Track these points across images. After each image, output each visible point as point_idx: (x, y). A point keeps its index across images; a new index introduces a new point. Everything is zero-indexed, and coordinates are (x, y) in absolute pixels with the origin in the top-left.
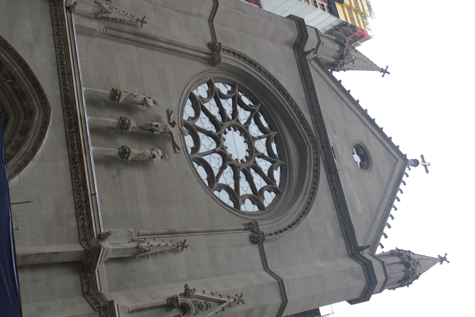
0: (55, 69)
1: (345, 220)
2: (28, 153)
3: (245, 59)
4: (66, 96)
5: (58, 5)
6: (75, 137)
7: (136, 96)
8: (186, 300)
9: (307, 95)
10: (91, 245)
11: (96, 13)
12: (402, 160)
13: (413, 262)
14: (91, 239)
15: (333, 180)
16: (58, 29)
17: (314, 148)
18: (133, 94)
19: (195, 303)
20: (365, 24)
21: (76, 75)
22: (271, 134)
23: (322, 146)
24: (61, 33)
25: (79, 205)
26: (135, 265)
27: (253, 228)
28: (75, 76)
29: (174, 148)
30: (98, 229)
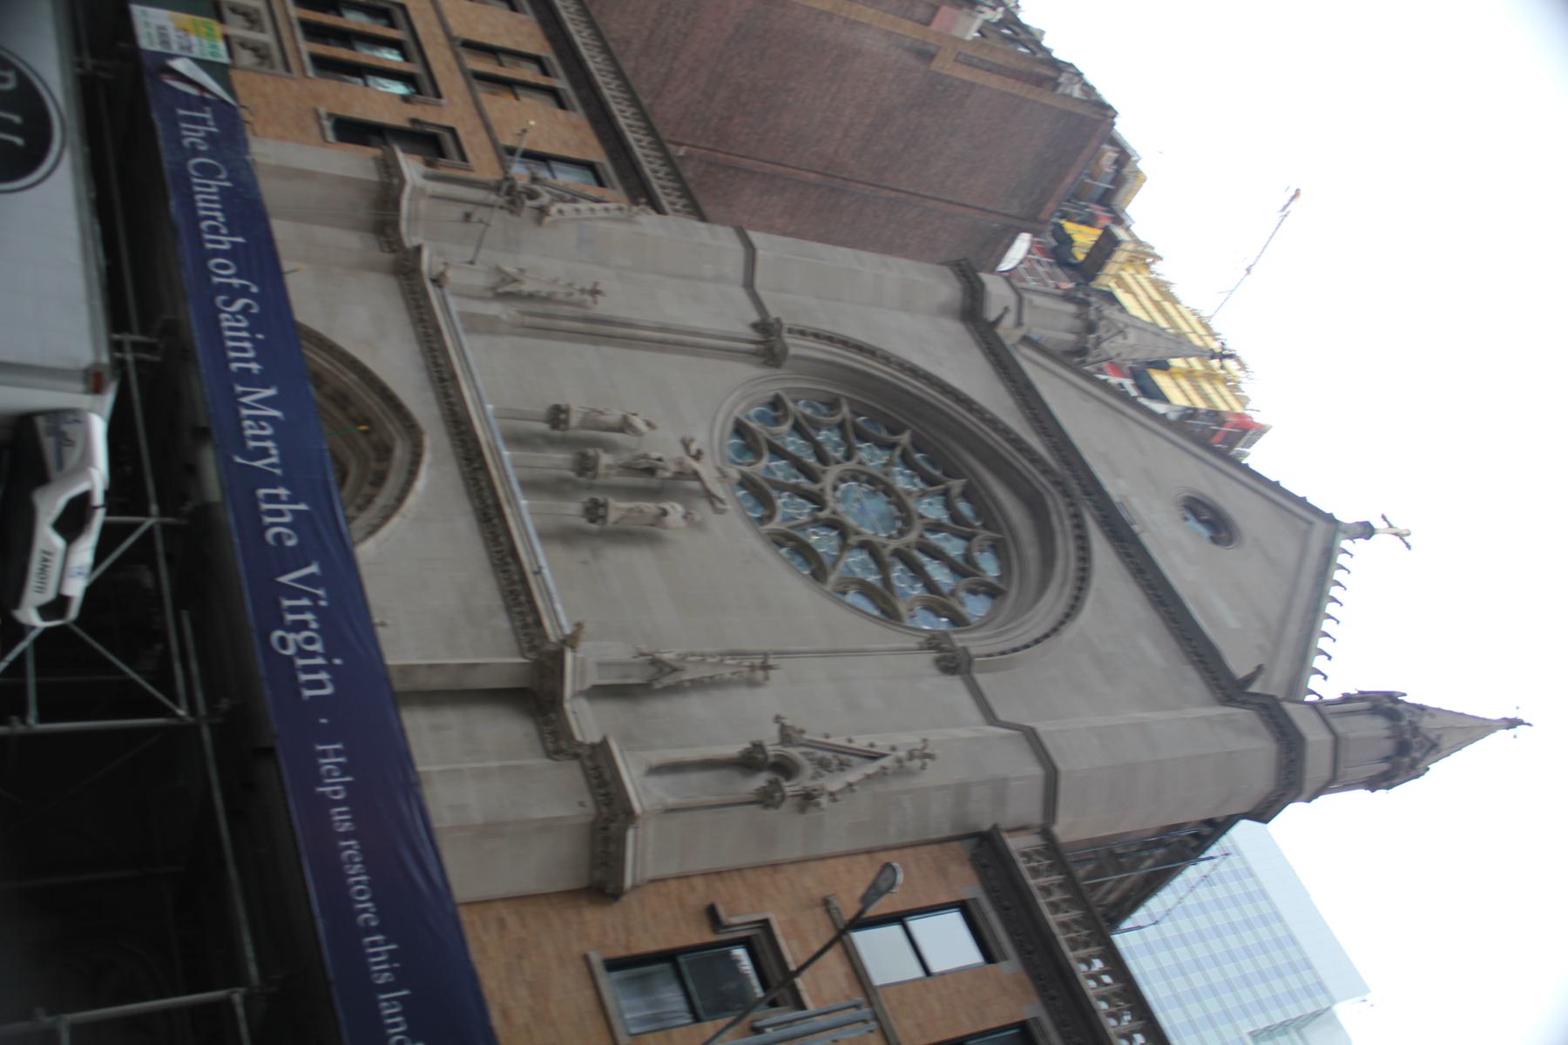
0: (423, 376)
3: (846, 343)
20: (1243, 401)
26: (658, 708)
29: (712, 503)
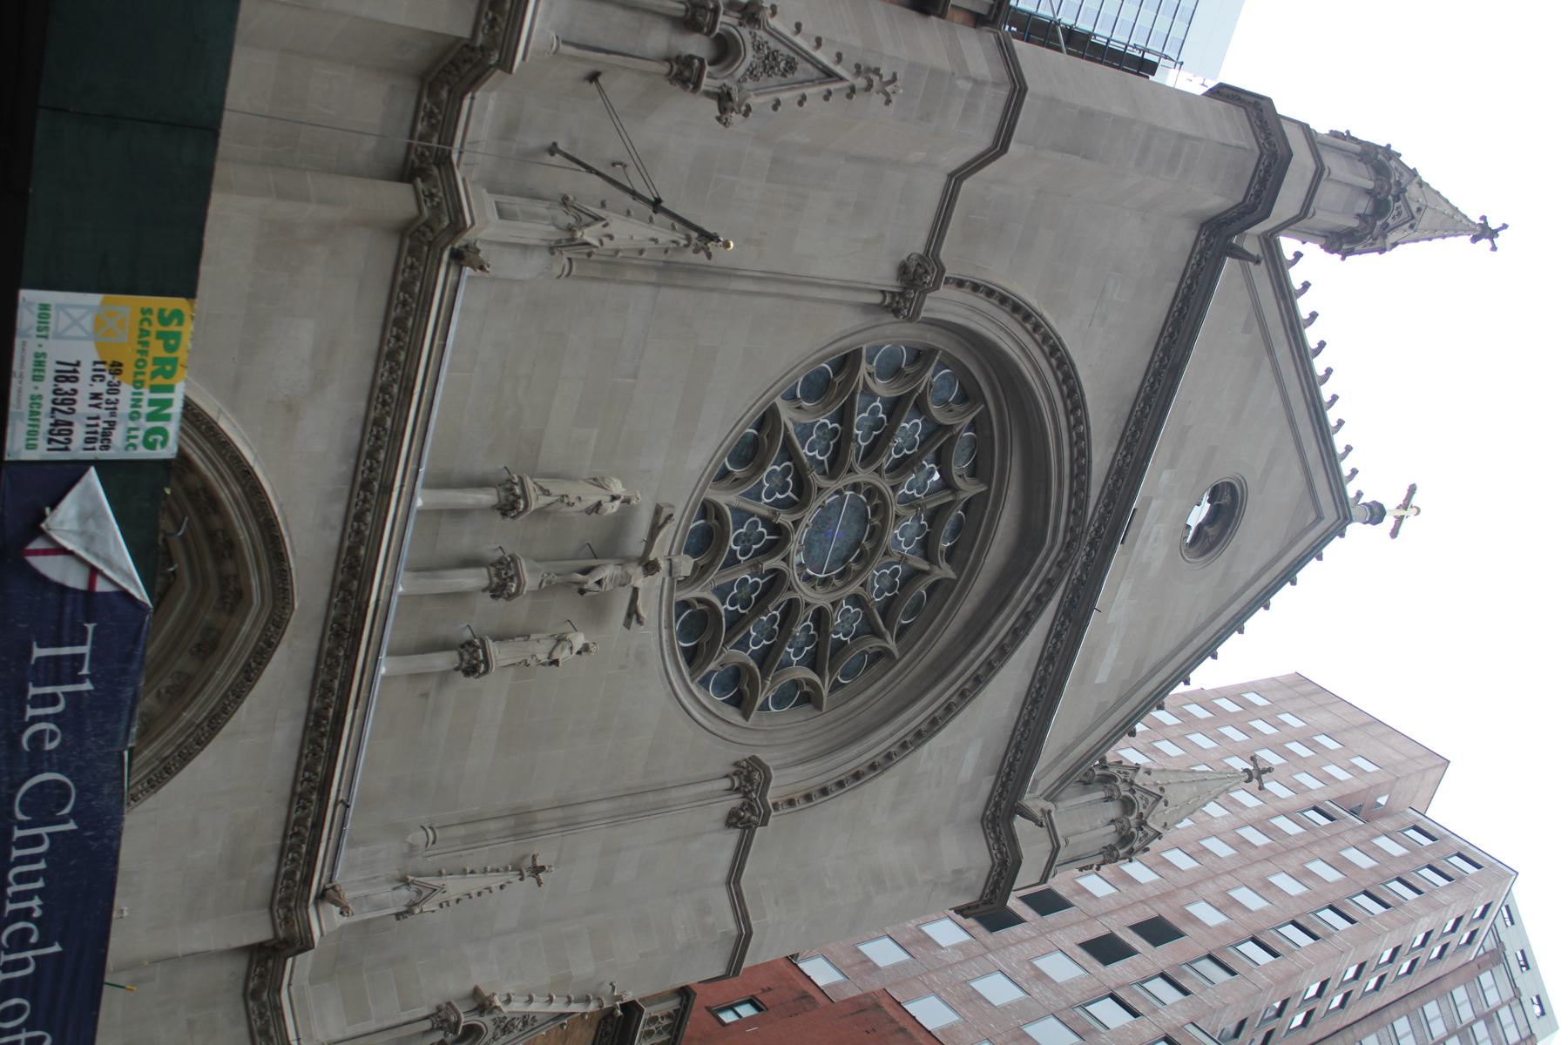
0: (346, 469)
1: (1026, 739)
2: (198, 726)
4: (353, 550)
5: (424, 256)
6: (339, 671)
7: (573, 504)
8: (481, 1019)
9: (1033, 690)
10: (293, 925)
11: (553, 244)
12: (1335, 517)
13: (1402, 208)
14: (300, 908)
16: (398, 338)
17: (1064, 548)
18: (567, 496)
19: (498, 1023)
21: (406, 483)
22: (936, 570)
23: (1093, 539)
24: (402, 357)
25: (296, 829)
27: (750, 792)
28: (329, 838)
29: (629, 615)
30: (326, 873)
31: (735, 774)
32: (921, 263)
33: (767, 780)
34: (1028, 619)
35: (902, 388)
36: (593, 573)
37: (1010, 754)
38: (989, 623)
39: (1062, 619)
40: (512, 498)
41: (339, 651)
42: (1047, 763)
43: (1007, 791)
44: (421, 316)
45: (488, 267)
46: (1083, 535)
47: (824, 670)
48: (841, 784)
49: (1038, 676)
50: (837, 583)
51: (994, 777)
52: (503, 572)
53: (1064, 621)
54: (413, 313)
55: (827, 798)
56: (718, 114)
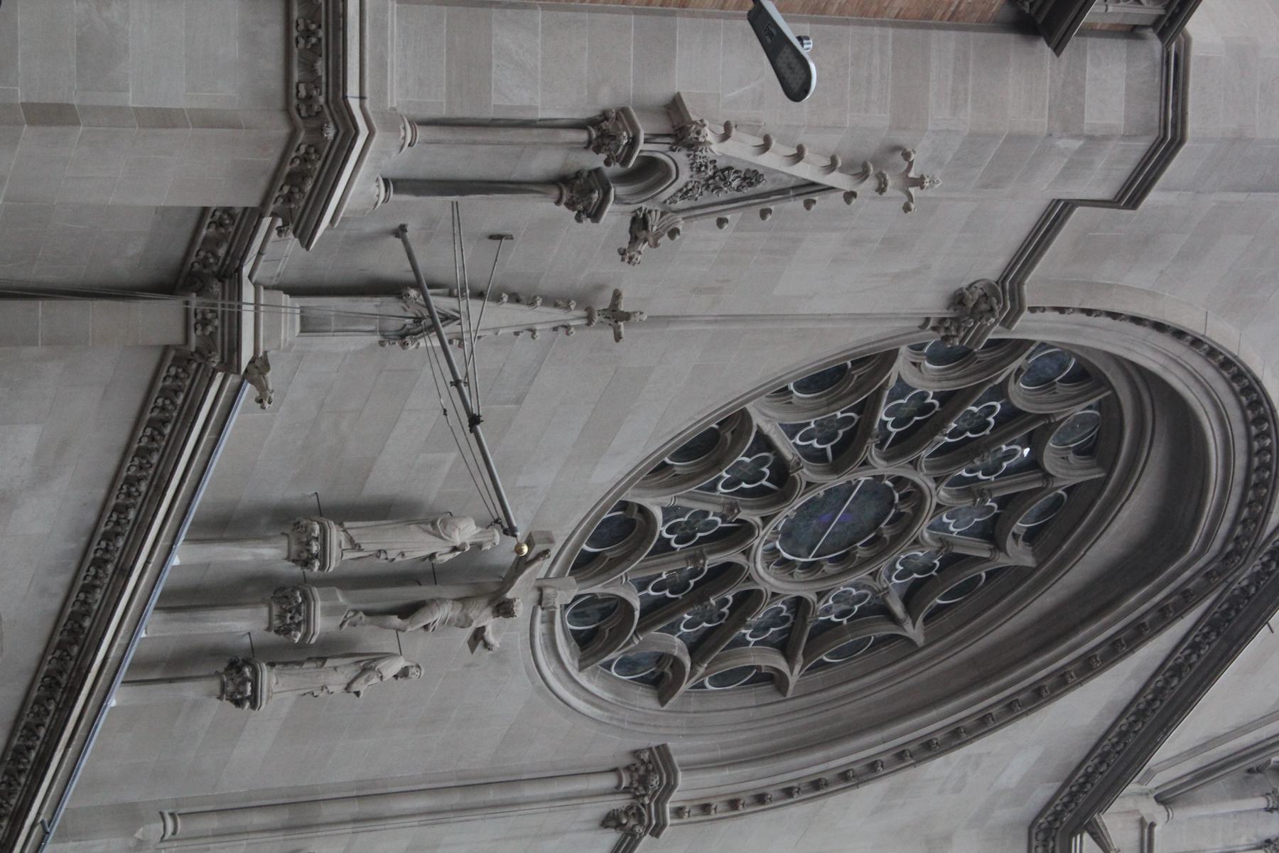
0: (77, 546)
4: (76, 618)
5: (192, 373)
6: (47, 721)
15: (1202, 652)
16: (152, 439)
17: (1221, 558)
21: (153, 560)
27: (644, 796)
31: (627, 768)
32: (988, 294)
33: (670, 788)
34: (1137, 635)
35: (968, 379)
36: (418, 616)
37: (1089, 763)
38: (1073, 630)
39: (1206, 630)
40: (305, 555)
41: (50, 705)
42: (1177, 752)
43: (1077, 804)
44: (183, 424)
45: (270, 403)
46: (1254, 551)
47: (795, 655)
48: (788, 792)
49: (1152, 686)
50: (829, 568)
51: (1058, 784)
52: (289, 615)
53: (1208, 633)
54: (173, 421)
55: (762, 807)
56: (626, 246)
